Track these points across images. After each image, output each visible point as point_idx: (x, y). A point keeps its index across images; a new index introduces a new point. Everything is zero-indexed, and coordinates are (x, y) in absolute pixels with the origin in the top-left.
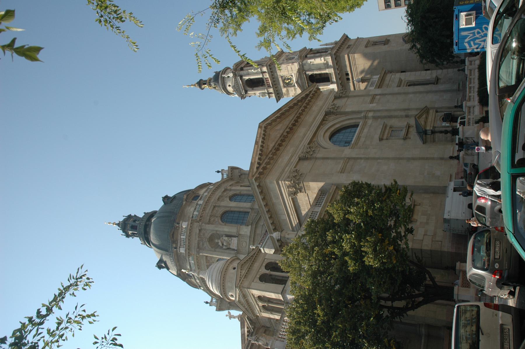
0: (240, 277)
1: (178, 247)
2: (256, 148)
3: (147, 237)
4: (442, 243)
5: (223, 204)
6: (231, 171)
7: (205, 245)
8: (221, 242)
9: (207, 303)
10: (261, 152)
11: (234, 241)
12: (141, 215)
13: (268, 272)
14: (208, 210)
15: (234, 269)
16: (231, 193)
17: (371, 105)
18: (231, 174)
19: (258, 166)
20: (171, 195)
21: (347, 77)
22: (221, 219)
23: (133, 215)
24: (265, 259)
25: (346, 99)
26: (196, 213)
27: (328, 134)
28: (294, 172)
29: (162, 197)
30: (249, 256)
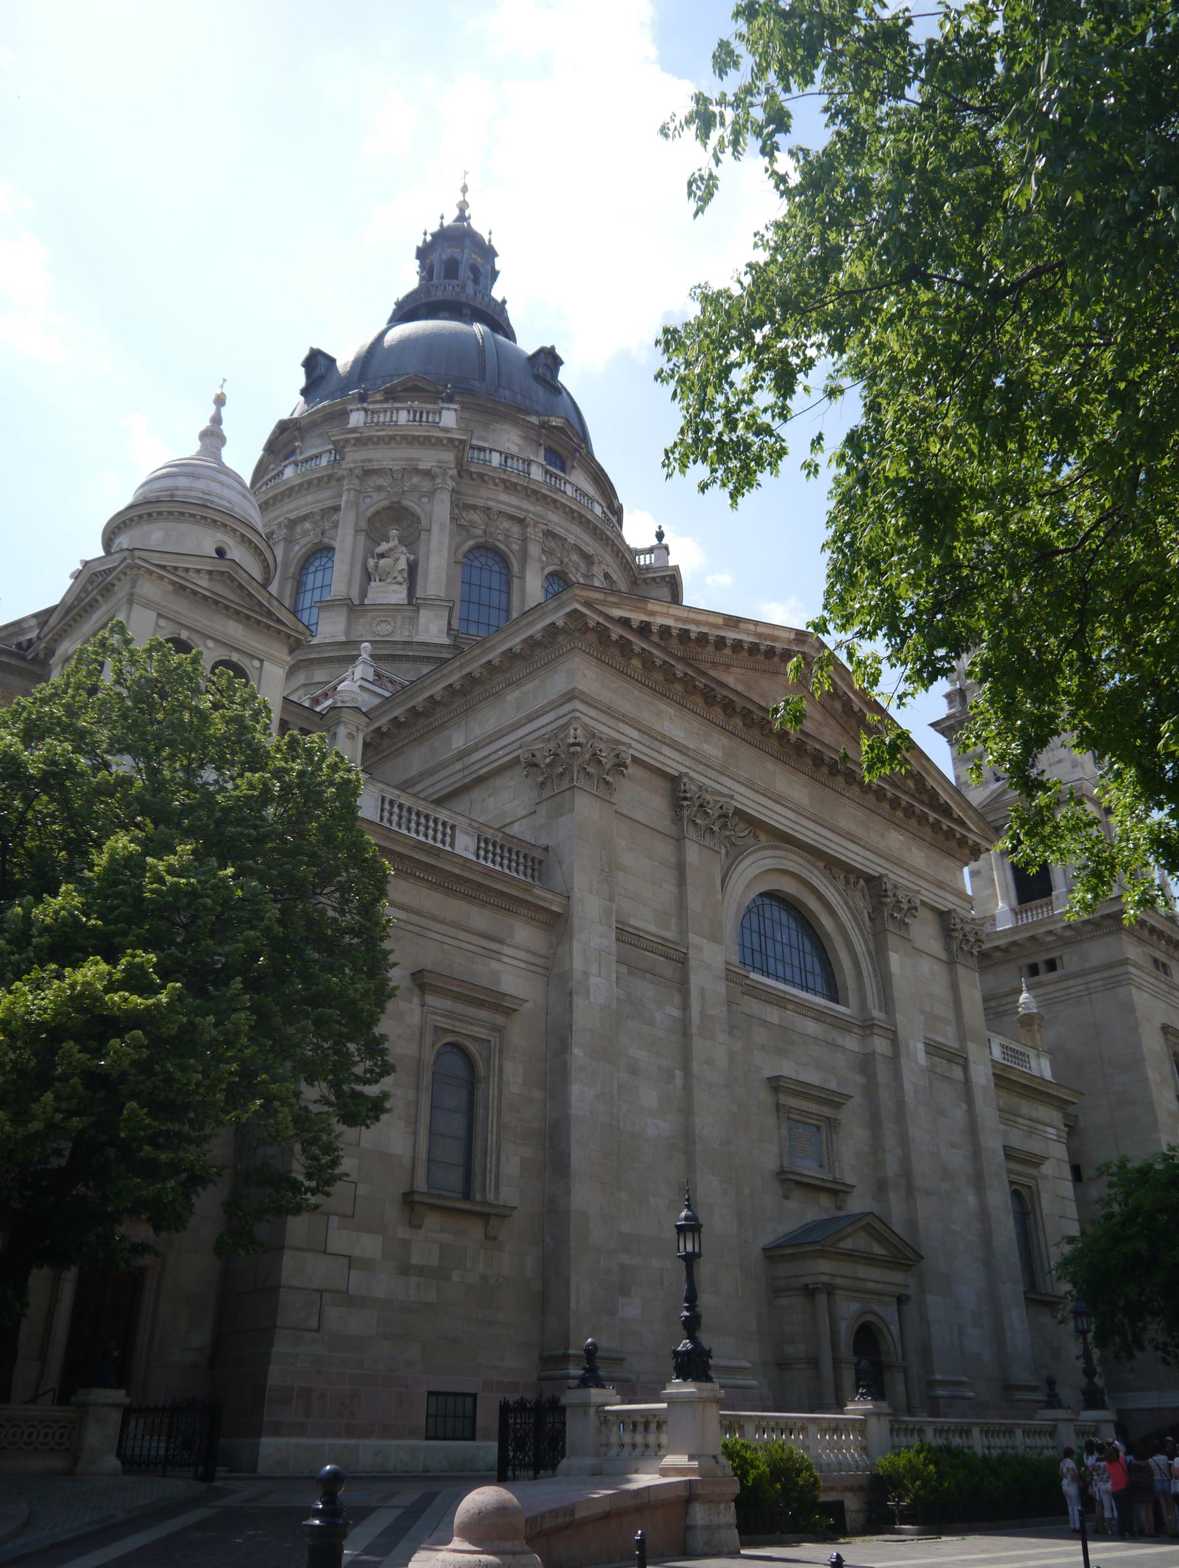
0: (176, 568)
2: (711, 619)
4: (310, 1330)
6: (663, 577)
7: (376, 496)
8: (391, 549)
10: (693, 636)
11: (396, 592)
12: (498, 292)
14: (508, 501)
17: (920, 1046)
18: (654, 579)
19: (635, 625)
20: (564, 377)
21: (1042, 967)
23: (499, 264)
24: (261, 661)
25: (942, 955)
26: (496, 459)
27: (788, 887)
28: (617, 756)
29: (553, 348)
30: (269, 602)
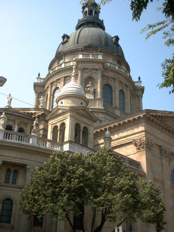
1: (83, 53)
3: (85, 24)
5: (117, 84)
6: (141, 89)
7: (86, 74)
8: (89, 86)
9: (39, 75)
10: (164, 116)
13: (82, 128)
14: (111, 75)
15: (81, 104)
16: (125, 90)
18: (139, 89)
19: (154, 116)
22: (106, 85)
24: (90, 126)
26: (109, 64)
29: (118, 36)
